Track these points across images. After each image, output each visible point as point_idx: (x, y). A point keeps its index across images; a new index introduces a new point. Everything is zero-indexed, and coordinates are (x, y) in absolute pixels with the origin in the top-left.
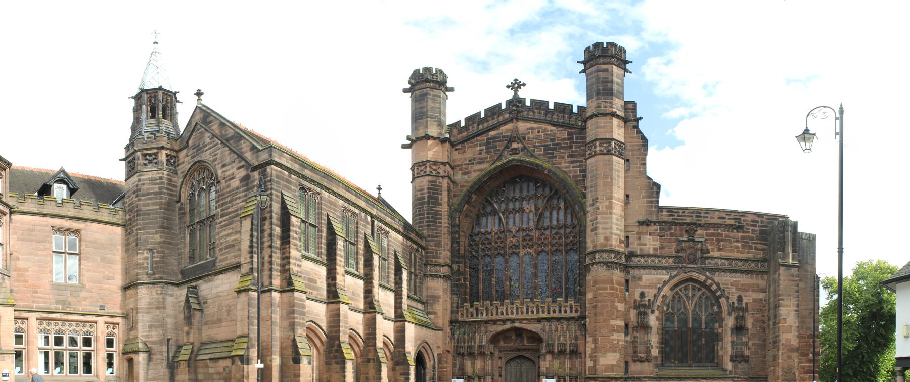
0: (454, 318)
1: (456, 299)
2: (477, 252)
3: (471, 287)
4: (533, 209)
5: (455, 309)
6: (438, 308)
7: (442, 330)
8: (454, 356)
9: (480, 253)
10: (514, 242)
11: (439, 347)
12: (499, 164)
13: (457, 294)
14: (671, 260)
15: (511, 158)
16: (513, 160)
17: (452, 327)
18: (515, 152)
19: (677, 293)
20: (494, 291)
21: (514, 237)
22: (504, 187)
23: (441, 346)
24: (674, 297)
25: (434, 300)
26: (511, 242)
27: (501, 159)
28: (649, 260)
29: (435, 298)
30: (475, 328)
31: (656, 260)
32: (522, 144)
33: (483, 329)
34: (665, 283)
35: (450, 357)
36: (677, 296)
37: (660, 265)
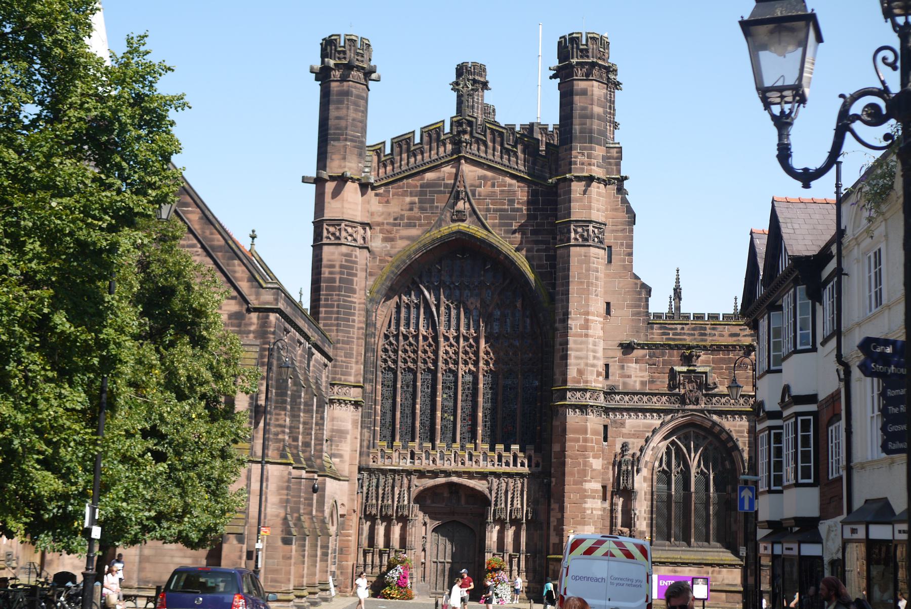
0: (363, 464)
1: (367, 434)
2: (395, 362)
3: (384, 414)
4: (478, 305)
5: (365, 449)
6: (344, 448)
7: (348, 481)
8: (360, 518)
9: (400, 363)
10: (451, 353)
11: (343, 504)
12: (436, 234)
13: (369, 428)
14: (664, 399)
15: (455, 227)
16: (459, 232)
17: (360, 476)
18: (459, 217)
19: (673, 443)
20: (418, 424)
21: (451, 345)
22: (440, 263)
23: (345, 503)
24: (668, 448)
25: (340, 437)
26: (447, 352)
27: (440, 226)
28: (636, 398)
29: (340, 434)
30: (394, 480)
31: (645, 399)
32: (471, 204)
33: (405, 481)
34: (654, 432)
35: (355, 519)
36: (673, 449)
37: (649, 406)
